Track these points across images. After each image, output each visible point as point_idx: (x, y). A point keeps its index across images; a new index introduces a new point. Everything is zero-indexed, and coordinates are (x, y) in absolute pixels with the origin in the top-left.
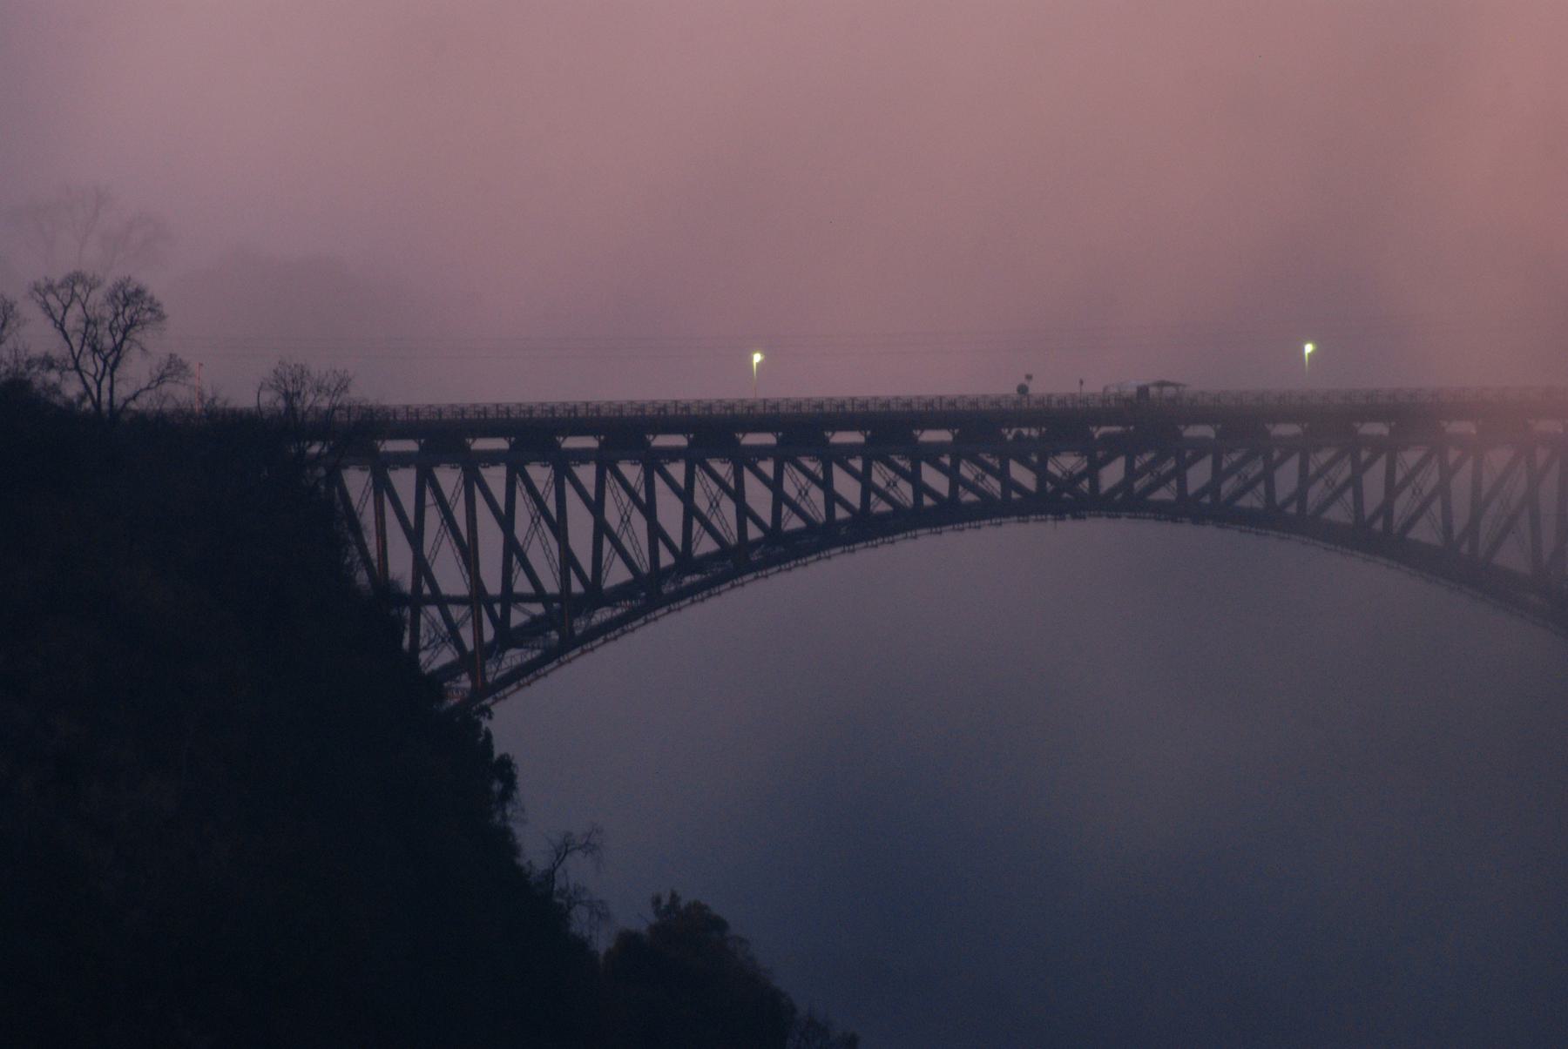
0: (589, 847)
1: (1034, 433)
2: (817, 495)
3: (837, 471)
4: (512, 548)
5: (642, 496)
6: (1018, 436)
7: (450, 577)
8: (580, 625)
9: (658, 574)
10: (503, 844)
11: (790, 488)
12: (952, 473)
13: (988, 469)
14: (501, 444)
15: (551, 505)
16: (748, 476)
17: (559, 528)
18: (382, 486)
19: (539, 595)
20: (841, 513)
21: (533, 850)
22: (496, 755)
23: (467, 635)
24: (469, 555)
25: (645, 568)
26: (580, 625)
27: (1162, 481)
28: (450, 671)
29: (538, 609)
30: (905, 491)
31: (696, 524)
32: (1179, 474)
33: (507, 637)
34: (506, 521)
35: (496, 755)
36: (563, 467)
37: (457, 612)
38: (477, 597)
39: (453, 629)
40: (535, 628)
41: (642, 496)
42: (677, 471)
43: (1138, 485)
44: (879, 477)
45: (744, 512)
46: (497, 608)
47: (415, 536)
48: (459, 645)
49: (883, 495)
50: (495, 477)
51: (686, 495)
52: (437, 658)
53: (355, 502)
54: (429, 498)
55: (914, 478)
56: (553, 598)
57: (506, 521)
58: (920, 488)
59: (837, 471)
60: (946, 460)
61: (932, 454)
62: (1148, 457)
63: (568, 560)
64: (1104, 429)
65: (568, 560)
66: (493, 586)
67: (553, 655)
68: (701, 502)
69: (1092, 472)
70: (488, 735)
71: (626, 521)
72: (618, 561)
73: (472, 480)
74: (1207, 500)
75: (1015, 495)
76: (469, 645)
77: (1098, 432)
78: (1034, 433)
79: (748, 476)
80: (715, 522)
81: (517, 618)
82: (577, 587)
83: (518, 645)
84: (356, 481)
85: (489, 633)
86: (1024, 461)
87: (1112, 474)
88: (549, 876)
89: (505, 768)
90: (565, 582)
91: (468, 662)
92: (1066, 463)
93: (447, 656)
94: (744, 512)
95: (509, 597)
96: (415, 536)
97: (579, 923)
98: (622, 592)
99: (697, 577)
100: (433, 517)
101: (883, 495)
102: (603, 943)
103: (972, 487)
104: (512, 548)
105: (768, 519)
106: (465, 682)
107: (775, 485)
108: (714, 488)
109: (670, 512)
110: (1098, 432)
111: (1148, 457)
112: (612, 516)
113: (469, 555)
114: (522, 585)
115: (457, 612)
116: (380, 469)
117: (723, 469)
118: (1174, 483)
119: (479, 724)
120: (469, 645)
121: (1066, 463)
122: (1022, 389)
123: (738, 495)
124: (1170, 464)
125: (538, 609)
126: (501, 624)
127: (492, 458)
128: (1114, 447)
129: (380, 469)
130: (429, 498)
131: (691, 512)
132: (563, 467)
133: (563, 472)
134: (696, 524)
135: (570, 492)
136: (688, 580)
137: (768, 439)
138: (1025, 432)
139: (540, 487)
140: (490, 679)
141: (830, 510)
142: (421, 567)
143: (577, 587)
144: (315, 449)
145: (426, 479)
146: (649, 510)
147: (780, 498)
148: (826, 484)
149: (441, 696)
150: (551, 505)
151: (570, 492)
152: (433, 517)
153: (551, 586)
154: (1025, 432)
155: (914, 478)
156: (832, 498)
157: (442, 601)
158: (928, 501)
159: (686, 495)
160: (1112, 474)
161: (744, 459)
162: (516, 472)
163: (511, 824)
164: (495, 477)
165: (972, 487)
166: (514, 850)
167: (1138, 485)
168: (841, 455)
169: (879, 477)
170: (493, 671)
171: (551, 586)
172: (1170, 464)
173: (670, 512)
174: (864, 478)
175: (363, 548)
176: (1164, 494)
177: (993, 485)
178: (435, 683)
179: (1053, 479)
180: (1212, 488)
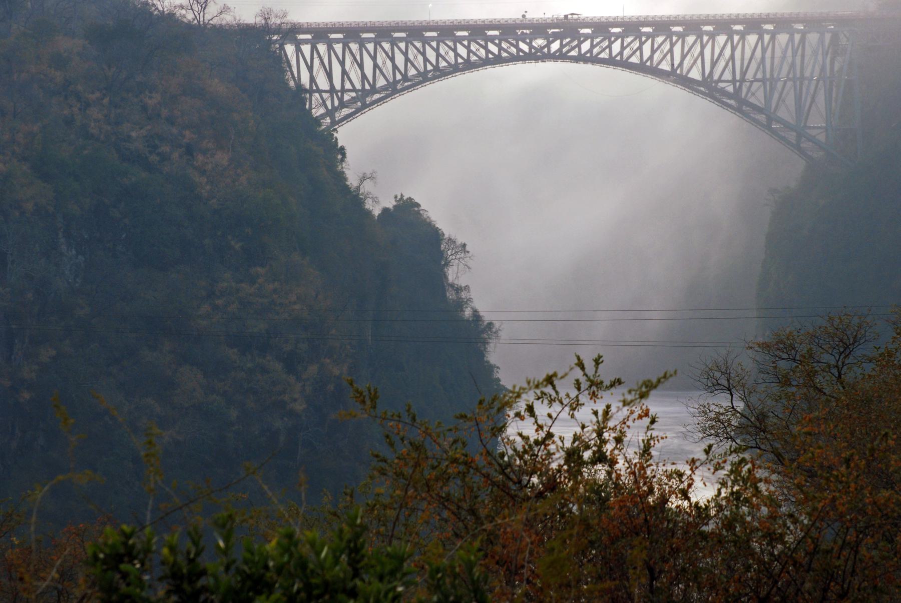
0: (372, 178)
1: (528, 32)
2: (451, 54)
3: (458, 45)
4: (344, 73)
5: (390, 54)
6: (522, 32)
7: (322, 83)
8: (368, 100)
9: (396, 82)
10: (341, 177)
11: (442, 52)
12: (499, 46)
13: (512, 45)
14: (340, 36)
15: (358, 58)
16: (427, 47)
17: (361, 66)
18: (299, 51)
19: (354, 89)
20: (460, 60)
21: (352, 180)
22: (339, 146)
23: (329, 103)
24: (329, 75)
25: (391, 80)
26: (368, 100)
27: (573, 49)
28: (323, 116)
29: (354, 94)
30: (482, 53)
31: (409, 64)
32: (579, 46)
33: (343, 105)
34: (342, 63)
35: (339, 146)
36: (362, 45)
37: (325, 95)
38: (332, 90)
39: (324, 102)
40: (353, 100)
41: (390, 54)
42: (402, 45)
43: (564, 50)
44: (474, 47)
45: (426, 60)
46: (339, 94)
47: (310, 68)
48: (326, 107)
49: (475, 54)
50: (338, 48)
51: (405, 54)
52: (318, 112)
53: (289, 57)
54: (315, 55)
55: (485, 48)
56: (359, 90)
57: (342, 63)
58: (488, 51)
59: (458, 45)
60: (497, 41)
61: (492, 39)
62: (568, 40)
63: (364, 77)
64: (552, 30)
65: (364, 77)
66: (338, 86)
67: (358, 111)
68: (411, 56)
69: (548, 46)
70: (337, 139)
71: (384, 63)
72: (382, 77)
73: (330, 48)
74: (588, 55)
75: (521, 54)
76: (330, 107)
77: (550, 31)
78: (528, 32)
79: (427, 47)
80: (415, 64)
81: (346, 97)
82: (367, 87)
83: (347, 107)
84: (290, 49)
85: (336, 103)
86: (524, 42)
87: (555, 46)
88: (358, 188)
89: (342, 151)
90: (363, 85)
91: (330, 113)
92: (539, 42)
93: (322, 111)
94: (426, 60)
95: (343, 90)
96: (310, 68)
97: (369, 205)
98: (384, 88)
99: (409, 83)
100: (317, 61)
101: (475, 54)
102: (377, 212)
103: (506, 51)
104: (344, 73)
105: (434, 63)
106: (328, 120)
107: (437, 50)
108: (415, 51)
109: (400, 59)
110: (550, 31)
111: (568, 40)
112: (379, 62)
113: (329, 75)
114: (348, 86)
115: (325, 95)
116: (298, 44)
117: (419, 45)
118: (577, 49)
119: (333, 135)
120: (330, 107)
121: (539, 42)
122: (524, 16)
123: (423, 54)
124: (576, 43)
125: (354, 94)
126: (341, 100)
127: (337, 41)
128: (556, 36)
129: (298, 44)
130: (315, 55)
131: (407, 60)
132: (362, 45)
133: (362, 46)
134: (409, 64)
135: (364, 52)
136: (406, 84)
137: (434, 34)
138: (525, 31)
139: (354, 51)
140: (337, 119)
141: (456, 60)
142: (312, 80)
143: (367, 87)
144: (275, 38)
145: (314, 48)
146: (392, 59)
147: (438, 55)
148: (454, 50)
149: (320, 125)
150: (358, 58)
151: (364, 52)
152: (317, 61)
153: (358, 86)
154: (525, 31)
155: (485, 48)
156: (457, 55)
157: (320, 91)
158: (490, 56)
159: (405, 54)
160: (555, 46)
161: (426, 41)
162: (346, 46)
163: (344, 170)
164: (338, 48)
165: (506, 51)
166: (346, 179)
167: (564, 50)
168: (460, 40)
169: (474, 47)
170: (338, 116)
171: (358, 86)
172: (576, 43)
173: (400, 59)
174: (468, 48)
175: (292, 74)
176: (574, 53)
177: (513, 50)
178: (317, 121)
179: (534, 48)
180: (590, 51)
